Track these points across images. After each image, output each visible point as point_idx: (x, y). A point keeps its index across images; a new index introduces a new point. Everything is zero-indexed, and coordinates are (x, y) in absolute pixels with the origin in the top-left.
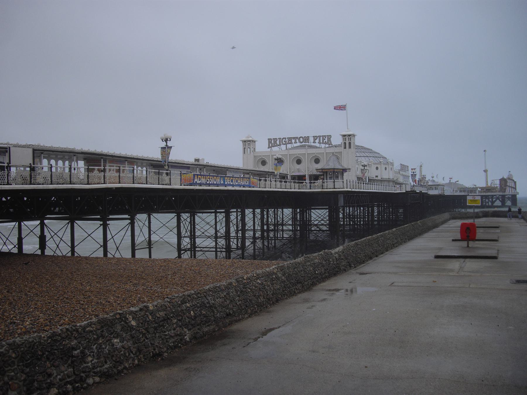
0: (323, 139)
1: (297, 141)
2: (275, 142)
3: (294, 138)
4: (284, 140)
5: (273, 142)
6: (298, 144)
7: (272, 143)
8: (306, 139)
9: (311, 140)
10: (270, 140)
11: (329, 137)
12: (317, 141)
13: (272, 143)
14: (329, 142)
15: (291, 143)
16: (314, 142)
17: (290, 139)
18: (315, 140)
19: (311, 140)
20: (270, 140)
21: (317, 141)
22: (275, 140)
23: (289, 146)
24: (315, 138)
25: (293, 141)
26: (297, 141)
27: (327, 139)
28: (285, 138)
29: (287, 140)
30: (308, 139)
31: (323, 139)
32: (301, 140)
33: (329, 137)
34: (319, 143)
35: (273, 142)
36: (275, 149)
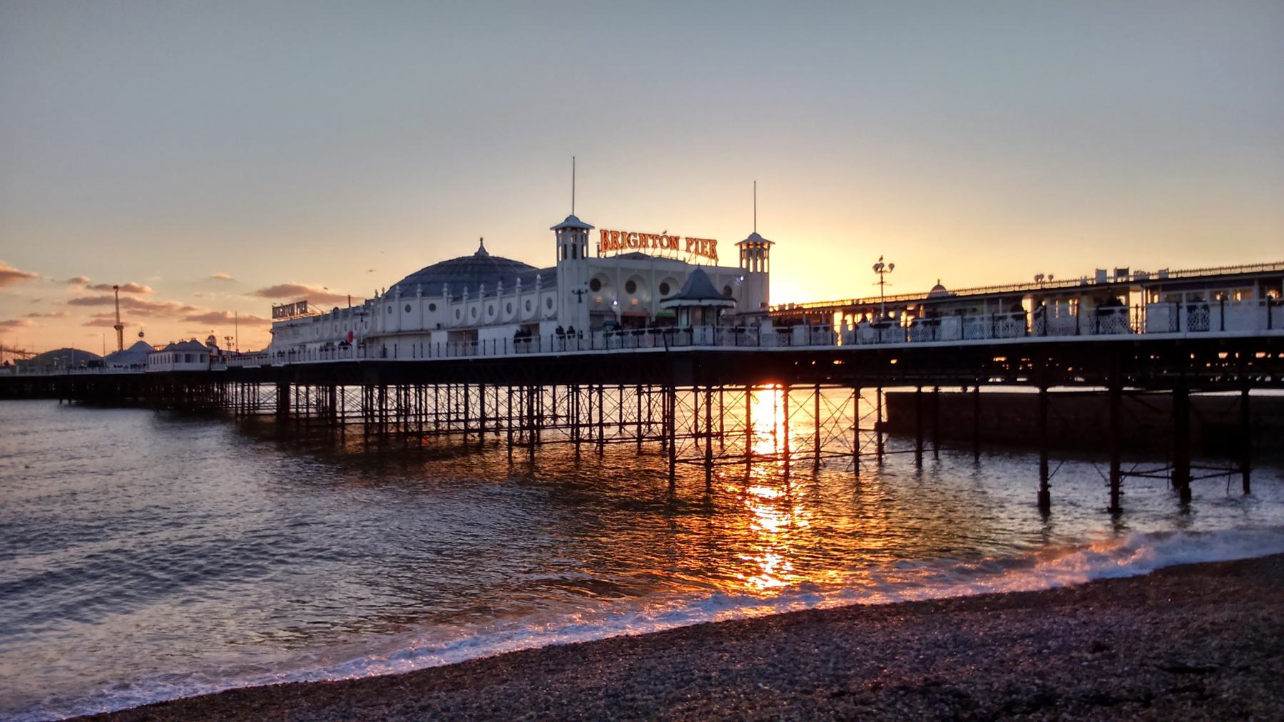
0: (703, 247)
2: (615, 239)
8: (673, 242)
10: (604, 234)
11: (713, 243)
12: (693, 248)
14: (713, 255)
15: (646, 246)
16: (688, 250)
18: (689, 245)
19: (683, 244)
20: (604, 234)
21: (693, 248)
22: (615, 234)
24: (690, 241)
25: (650, 242)
27: (709, 246)
28: (635, 234)
31: (703, 247)
32: (665, 242)
33: (713, 243)
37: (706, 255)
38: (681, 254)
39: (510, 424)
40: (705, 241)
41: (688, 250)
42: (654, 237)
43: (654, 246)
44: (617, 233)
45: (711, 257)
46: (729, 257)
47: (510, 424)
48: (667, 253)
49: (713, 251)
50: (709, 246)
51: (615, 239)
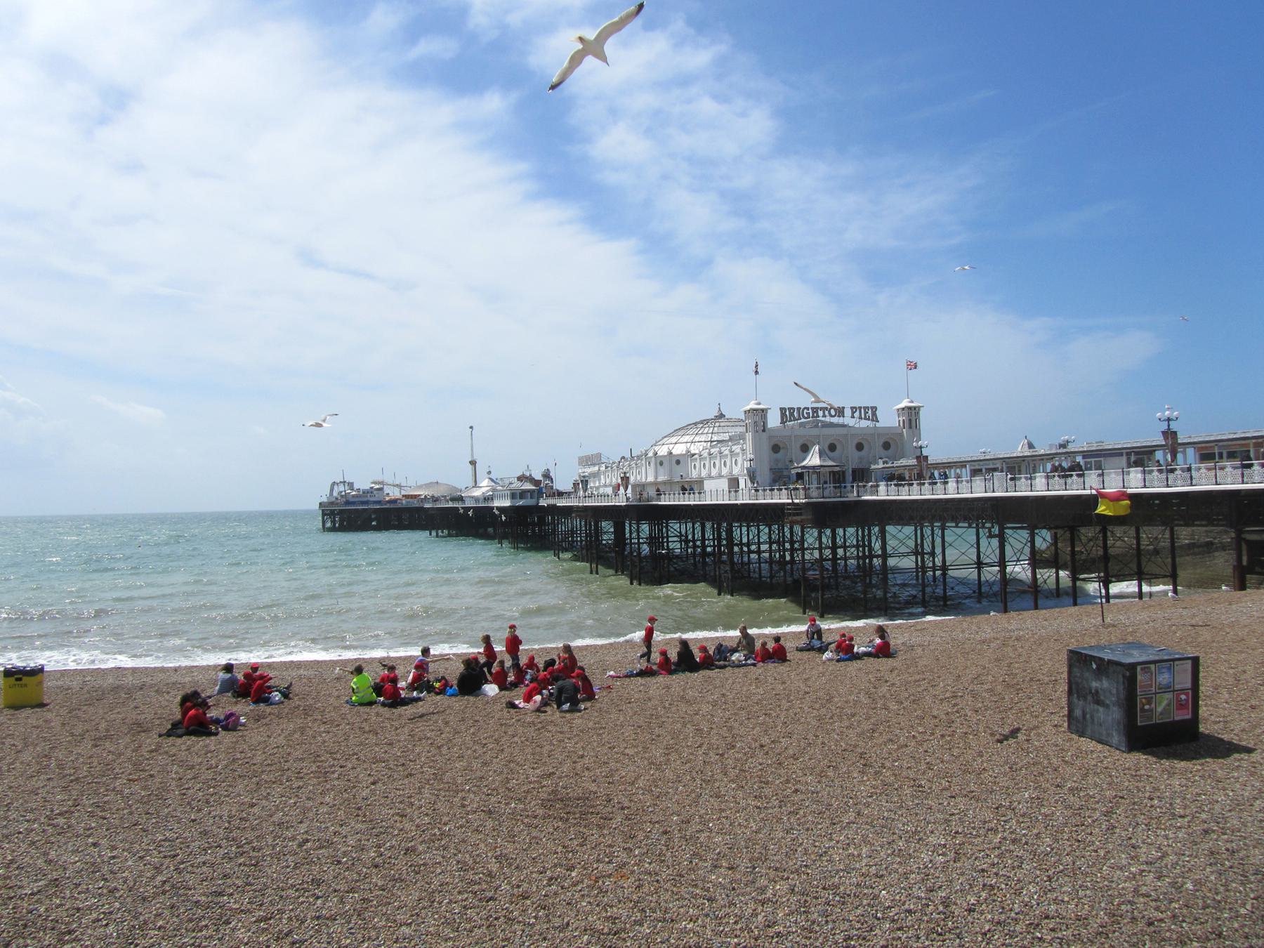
2: (792, 414)
8: (840, 412)
9: (848, 412)
10: (783, 410)
11: (874, 409)
12: (857, 414)
14: (875, 418)
16: (853, 417)
19: (848, 412)
20: (783, 410)
21: (857, 414)
24: (854, 409)
25: (821, 413)
27: (871, 413)
32: (833, 412)
33: (874, 409)
38: (847, 420)
39: (834, 553)
41: (853, 417)
43: (824, 416)
46: (889, 419)
47: (834, 553)
48: (835, 420)
49: (874, 414)
50: (871, 413)
51: (792, 414)
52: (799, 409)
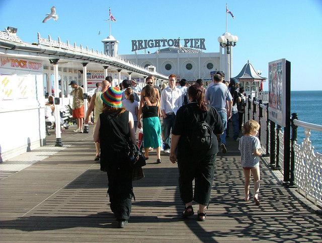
0: (196, 43)
1: (166, 43)
2: (140, 44)
3: (162, 41)
4: (150, 42)
5: (137, 44)
6: (167, 47)
7: (137, 45)
8: (176, 42)
11: (202, 41)
12: (189, 45)
13: (137, 45)
16: (186, 46)
17: (158, 42)
18: (186, 43)
19: (182, 44)
21: (189, 45)
22: (140, 42)
23: (157, 48)
24: (186, 41)
25: (161, 44)
26: (166, 43)
29: (154, 42)
30: (179, 43)
31: (196, 43)
32: (171, 43)
34: (191, 46)
35: (137, 44)
36: (139, 52)
37: (198, 47)
40: (198, 40)
42: (164, 41)
44: (142, 41)
45: (201, 48)
46: (212, 48)
52: (146, 41)
